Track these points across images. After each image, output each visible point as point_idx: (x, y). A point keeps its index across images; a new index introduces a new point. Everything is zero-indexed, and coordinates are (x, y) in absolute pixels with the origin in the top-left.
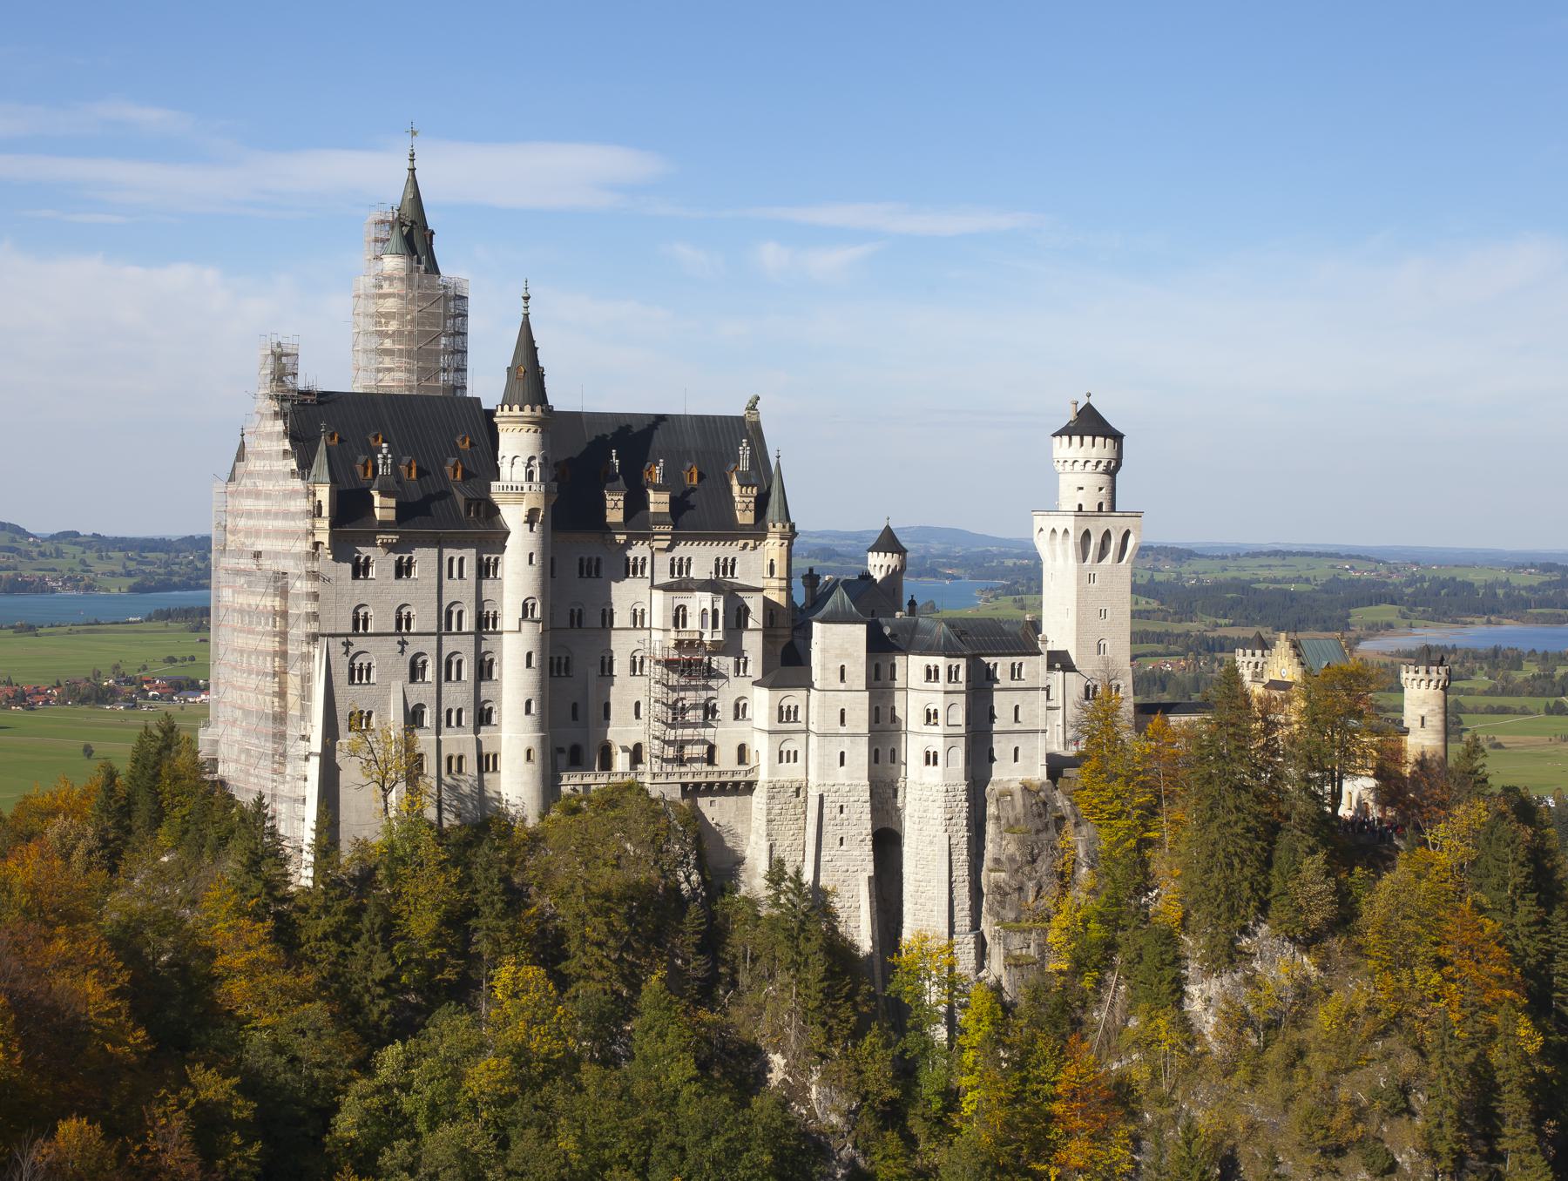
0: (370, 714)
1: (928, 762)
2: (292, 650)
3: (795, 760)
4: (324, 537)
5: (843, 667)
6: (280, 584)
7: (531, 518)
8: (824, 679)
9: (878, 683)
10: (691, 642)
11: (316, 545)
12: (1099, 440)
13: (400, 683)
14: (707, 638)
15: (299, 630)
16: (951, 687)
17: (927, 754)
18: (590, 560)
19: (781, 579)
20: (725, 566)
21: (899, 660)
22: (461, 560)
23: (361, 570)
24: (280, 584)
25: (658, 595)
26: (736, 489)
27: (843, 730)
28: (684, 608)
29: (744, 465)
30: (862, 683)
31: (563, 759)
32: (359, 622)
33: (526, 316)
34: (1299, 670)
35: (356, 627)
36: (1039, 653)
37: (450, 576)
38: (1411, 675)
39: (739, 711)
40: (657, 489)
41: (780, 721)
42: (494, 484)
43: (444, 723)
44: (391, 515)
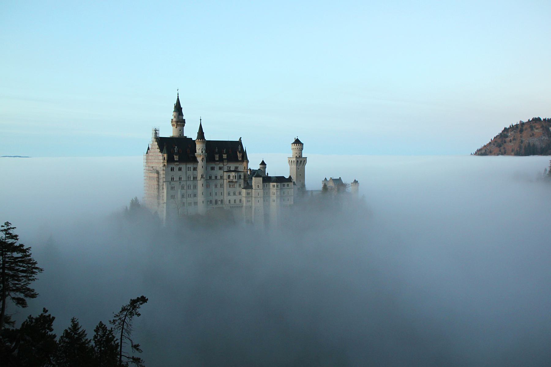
0: (174, 195)
1: (273, 202)
2: (161, 184)
3: (250, 202)
4: (166, 164)
5: (258, 185)
6: (158, 173)
7: (202, 160)
8: (255, 187)
9: (264, 188)
10: (231, 181)
11: (164, 165)
12: (299, 145)
13: (180, 190)
14: (234, 180)
15: (161, 181)
16: (277, 188)
17: (273, 200)
18: (213, 167)
19: (246, 170)
20: (236, 168)
21: (268, 184)
22: (190, 167)
23: (172, 169)
24: (158, 173)
25: (225, 173)
26: (238, 154)
27: (258, 196)
28: (230, 176)
29: (240, 150)
30: (262, 188)
31: (209, 203)
32: (172, 179)
33: (201, 123)
34: (334, 184)
35: (172, 180)
36: (292, 182)
37: (188, 170)
38: (353, 184)
39: (240, 193)
40: (224, 154)
41: (247, 195)
42: (195, 154)
43: (188, 197)
44: (177, 159)
